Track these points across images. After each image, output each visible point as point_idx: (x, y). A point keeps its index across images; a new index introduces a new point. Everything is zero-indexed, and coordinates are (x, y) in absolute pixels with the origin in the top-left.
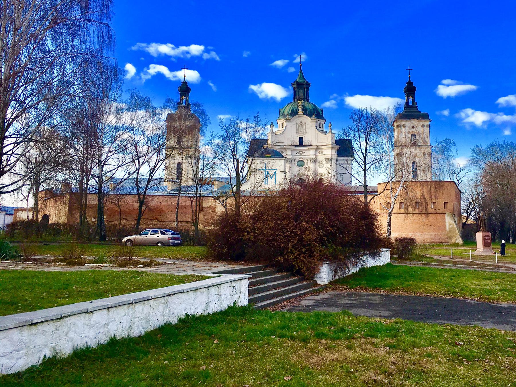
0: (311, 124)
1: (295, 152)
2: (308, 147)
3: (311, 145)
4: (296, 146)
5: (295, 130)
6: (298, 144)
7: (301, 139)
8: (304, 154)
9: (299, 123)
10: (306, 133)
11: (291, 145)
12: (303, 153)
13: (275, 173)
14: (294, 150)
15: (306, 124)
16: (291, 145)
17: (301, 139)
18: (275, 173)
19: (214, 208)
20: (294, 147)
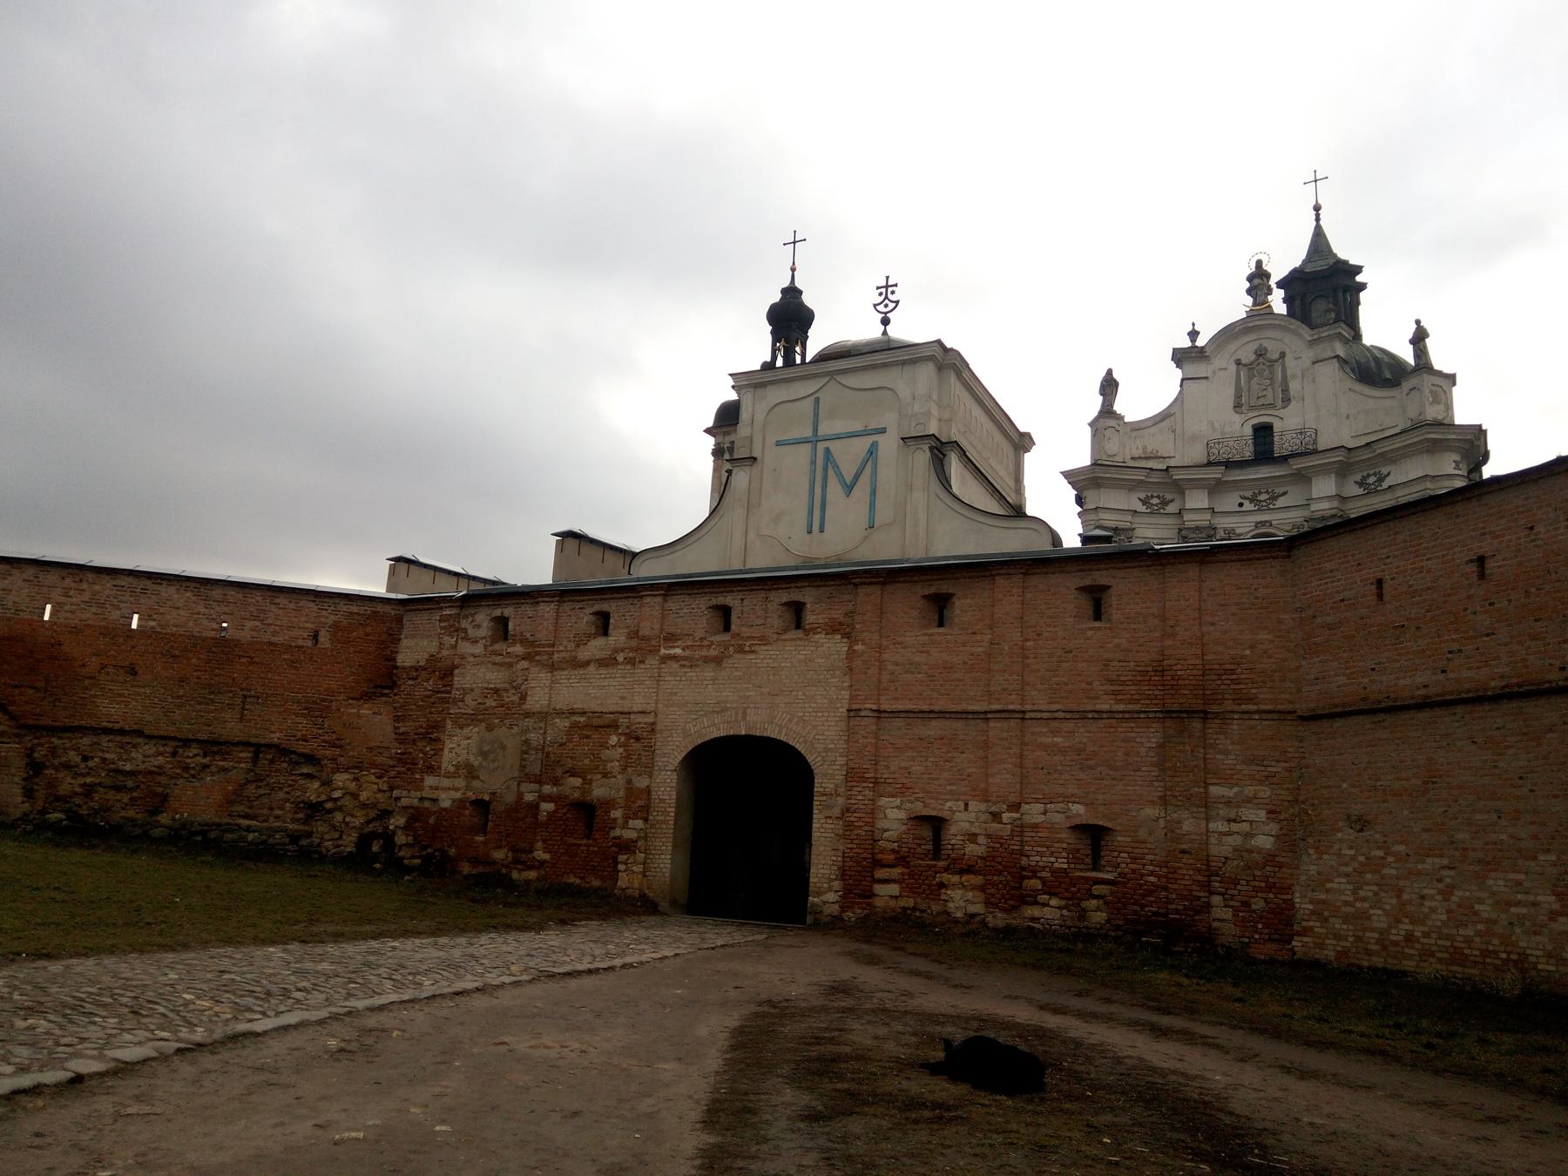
0: (1308, 355)
1: (1230, 502)
2: (1297, 464)
3: (1315, 452)
4: (1229, 465)
5: (1231, 392)
6: (1248, 453)
7: (1263, 432)
8: (1281, 502)
9: (1247, 355)
10: (1287, 400)
11: (1209, 464)
12: (1274, 498)
13: (874, 445)
14: (1216, 488)
15: (1289, 360)
16: (1209, 464)
17: (1263, 432)
18: (874, 445)
19: (447, 674)
20: (1216, 473)
